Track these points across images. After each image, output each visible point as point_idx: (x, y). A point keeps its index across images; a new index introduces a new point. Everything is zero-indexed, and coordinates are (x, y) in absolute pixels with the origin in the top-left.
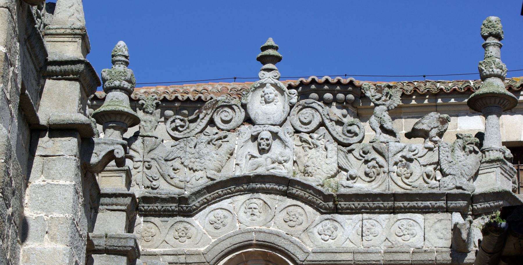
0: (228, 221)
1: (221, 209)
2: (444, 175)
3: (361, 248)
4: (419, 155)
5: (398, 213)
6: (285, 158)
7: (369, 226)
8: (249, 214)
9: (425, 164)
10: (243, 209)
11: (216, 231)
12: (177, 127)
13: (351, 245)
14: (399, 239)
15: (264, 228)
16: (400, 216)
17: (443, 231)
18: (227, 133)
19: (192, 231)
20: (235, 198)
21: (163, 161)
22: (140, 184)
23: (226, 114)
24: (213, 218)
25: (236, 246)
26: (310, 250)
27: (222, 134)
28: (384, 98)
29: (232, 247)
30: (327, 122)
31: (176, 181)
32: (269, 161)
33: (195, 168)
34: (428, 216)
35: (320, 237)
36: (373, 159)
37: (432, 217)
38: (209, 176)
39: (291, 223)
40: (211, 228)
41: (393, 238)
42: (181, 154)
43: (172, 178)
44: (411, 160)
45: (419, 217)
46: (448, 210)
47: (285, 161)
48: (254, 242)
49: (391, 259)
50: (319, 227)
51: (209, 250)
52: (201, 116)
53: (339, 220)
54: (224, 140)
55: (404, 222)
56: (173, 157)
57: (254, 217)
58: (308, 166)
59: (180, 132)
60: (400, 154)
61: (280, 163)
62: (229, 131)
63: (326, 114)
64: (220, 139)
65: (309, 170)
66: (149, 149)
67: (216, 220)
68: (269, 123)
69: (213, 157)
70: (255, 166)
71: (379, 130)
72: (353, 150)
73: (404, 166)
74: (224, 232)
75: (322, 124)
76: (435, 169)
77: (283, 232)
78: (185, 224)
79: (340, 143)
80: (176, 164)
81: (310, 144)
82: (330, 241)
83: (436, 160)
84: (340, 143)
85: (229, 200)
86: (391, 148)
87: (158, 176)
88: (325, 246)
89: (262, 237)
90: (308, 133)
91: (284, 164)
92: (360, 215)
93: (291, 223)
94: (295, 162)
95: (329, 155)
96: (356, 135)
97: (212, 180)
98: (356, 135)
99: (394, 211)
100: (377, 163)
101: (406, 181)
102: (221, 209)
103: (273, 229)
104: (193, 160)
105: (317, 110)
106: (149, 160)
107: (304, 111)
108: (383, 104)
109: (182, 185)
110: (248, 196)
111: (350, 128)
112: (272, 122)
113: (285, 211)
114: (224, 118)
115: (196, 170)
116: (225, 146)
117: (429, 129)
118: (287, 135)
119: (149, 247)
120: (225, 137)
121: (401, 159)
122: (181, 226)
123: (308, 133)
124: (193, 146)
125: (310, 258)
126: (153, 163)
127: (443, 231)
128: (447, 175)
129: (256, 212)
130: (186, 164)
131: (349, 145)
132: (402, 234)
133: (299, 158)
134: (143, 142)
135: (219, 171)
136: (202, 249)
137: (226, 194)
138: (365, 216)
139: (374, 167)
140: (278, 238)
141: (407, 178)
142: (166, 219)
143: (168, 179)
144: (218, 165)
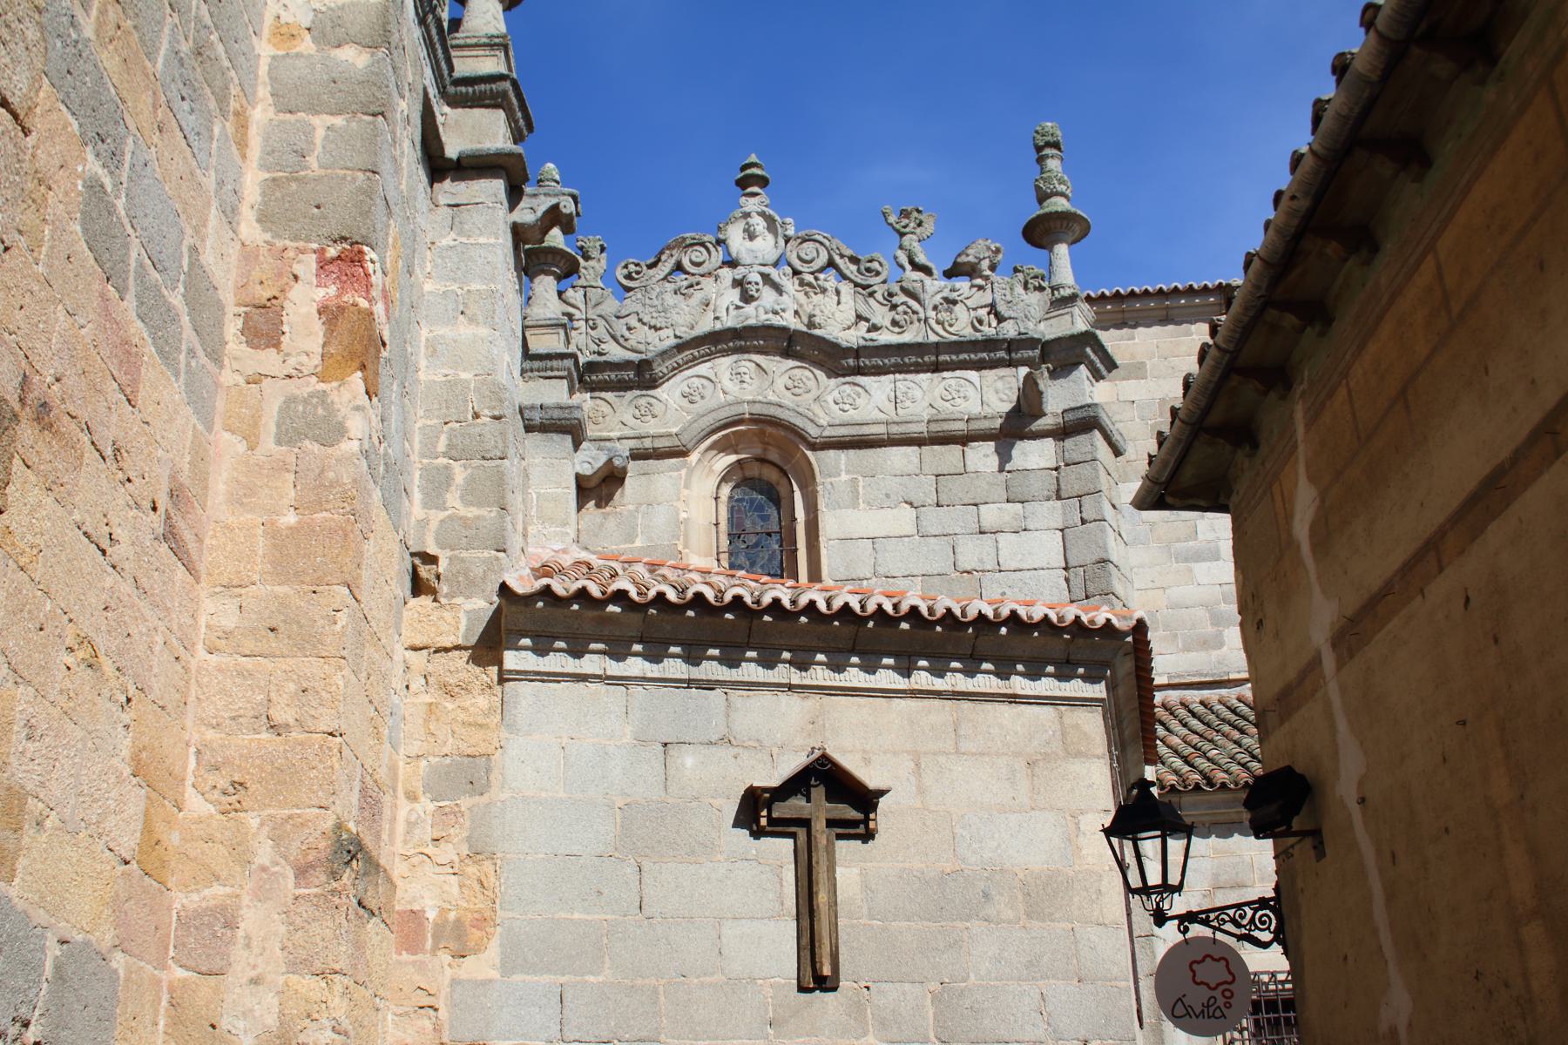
0: (708, 392)
1: (698, 376)
2: (1001, 319)
3: (896, 419)
4: (965, 295)
5: (943, 370)
6: (782, 306)
7: (904, 389)
8: (737, 381)
9: (974, 306)
10: (727, 375)
11: (692, 406)
12: (630, 273)
13: (882, 417)
14: (947, 404)
15: (760, 398)
16: (946, 374)
17: (1007, 392)
18: (701, 279)
19: (658, 408)
20: (718, 361)
21: (614, 319)
22: (584, 348)
23: (698, 254)
24: (687, 390)
25: (722, 422)
26: (825, 424)
27: (693, 280)
28: (912, 225)
29: (717, 424)
30: (837, 259)
31: (632, 343)
32: (761, 311)
33: (658, 325)
34: (985, 372)
35: (837, 407)
36: (902, 304)
37: (990, 375)
38: (678, 334)
39: (797, 391)
40: (685, 403)
41: (939, 403)
42: (639, 308)
43: (626, 340)
44: (954, 302)
45: (972, 375)
46: (1011, 364)
47: (783, 310)
48: (747, 416)
49: (939, 429)
50: (835, 394)
51: (684, 429)
52: (664, 258)
53: (862, 383)
54: (696, 287)
55: (953, 382)
56: (627, 313)
57: (745, 385)
58: (814, 316)
59: (637, 279)
60: (940, 295)
61: (776, 313)
62: (702, 276)
63: (834, 247)
64: (691, 286)
65: (817, 320)
66: (593, 303)
67: (692, 391)
68: (757, 262)
69: (682, 310)
70: (741, 318)
71: (908, 267)
72: (875, 292)
73: (946, 310)
74: (701, 406)
75: (831, 264)
76: (989, 313)
77: (785, 402)
78: (649, 398)
79: (856, 285)
80: (633, 321)
81: (814, 288)
82: (852, 412)
83: (990, 301)
84: (856, 285)
85: (708, 364)
86: (927, 287)
87: (608, 338)
88: (846, 417)
89: (757, 409)
90: (812, 273)
91: (782, 314)
92: (891, 376)
93: (797, 391)
94: (796, 312)
95: (843, 299)
96: (878, 273)
97: (680, 338)
98: (878, 273)
99: (937, 368)
100: (909, 307)
101: (951, 330)
102: (698, 376)
103: (772, 398)
104: (655, 315)
105: (821, 243)
106: (595, 317)
107: (805, 245)
108: (912, 233)
109: (642, 347)
110: (735, 357)
111: (869, 265)
112: (762, 262)
113: (787, 376)
114: (694, 259)
115: (660, 329)
116: (698, 296)
117: (976, 261)
118: (783, 277)
119: (600, 431)
120: (698, 284)
121: (942, 301)
122: (643, 401)
123: (812, 273)
124: (654, 297)
125: (826, 433)
126: (601, 322)
127: (1007, 392)
128: (1005, 319)
129: (746, 378)
130: (645, 320)
131: (871, 286)
132: (950, 397)
133: (801, 306)
134: (585, 296)
135: (692, 328)
136: (674, 430)
137: (703, 356)
138: (898, 376)
139: (905, 313)
140: (780, 410)
141: (951, 325)
142: (622, 393)
143: (621, 341)
144: (689, 319)
